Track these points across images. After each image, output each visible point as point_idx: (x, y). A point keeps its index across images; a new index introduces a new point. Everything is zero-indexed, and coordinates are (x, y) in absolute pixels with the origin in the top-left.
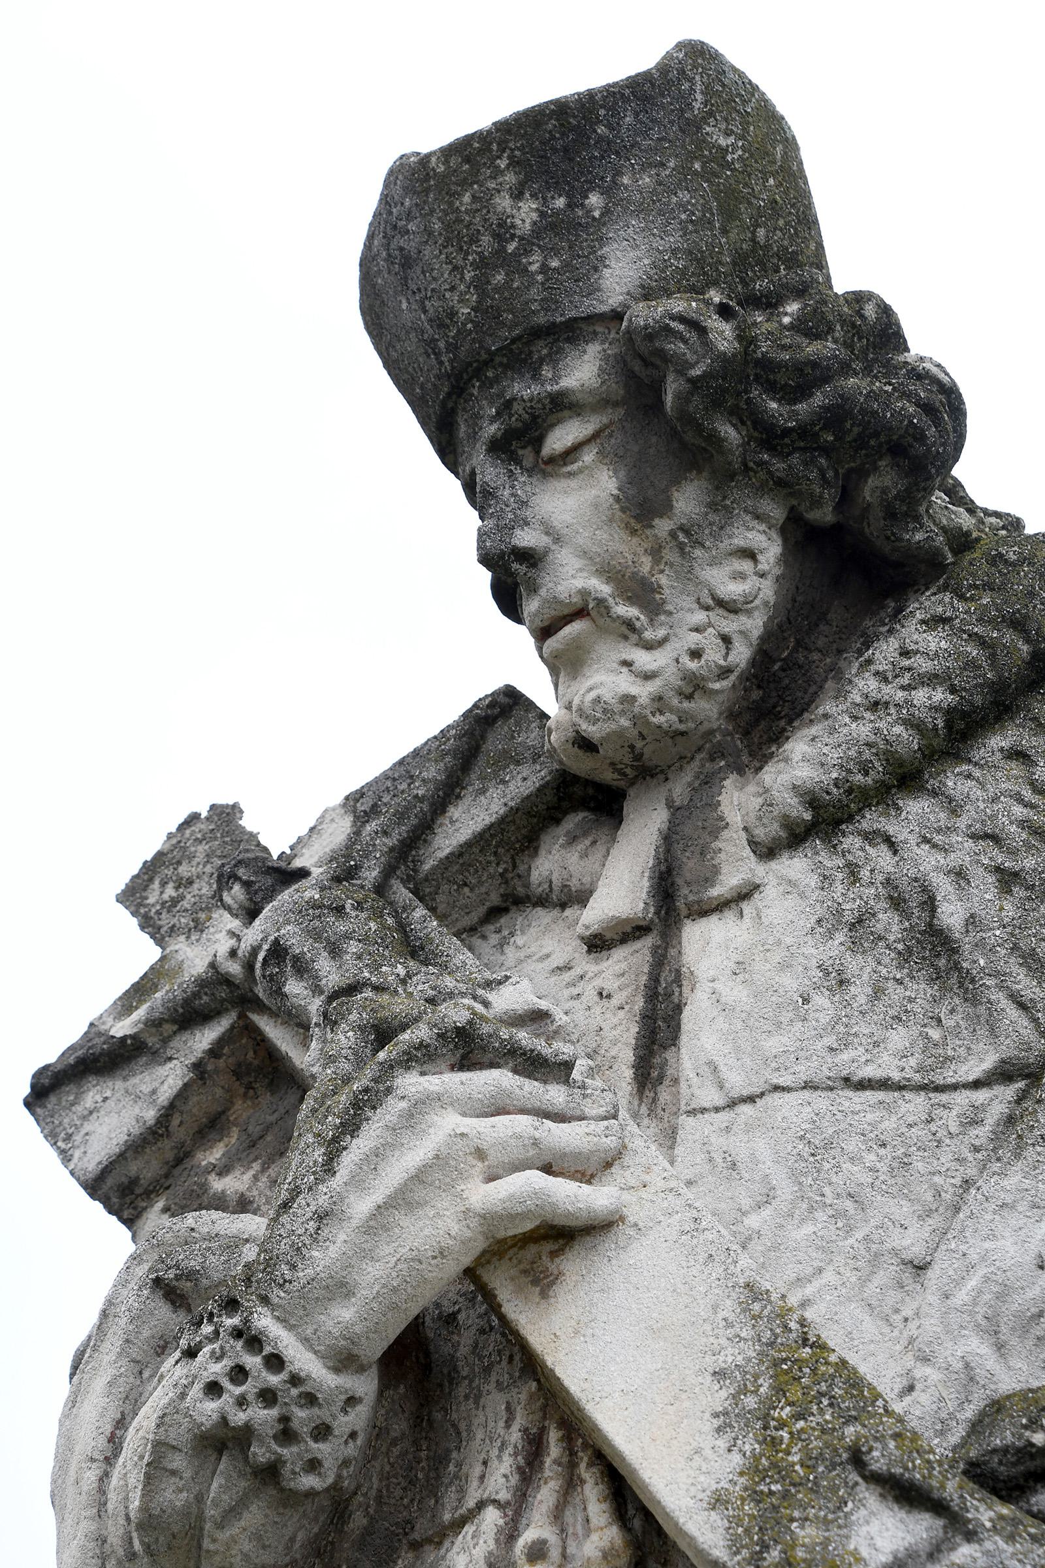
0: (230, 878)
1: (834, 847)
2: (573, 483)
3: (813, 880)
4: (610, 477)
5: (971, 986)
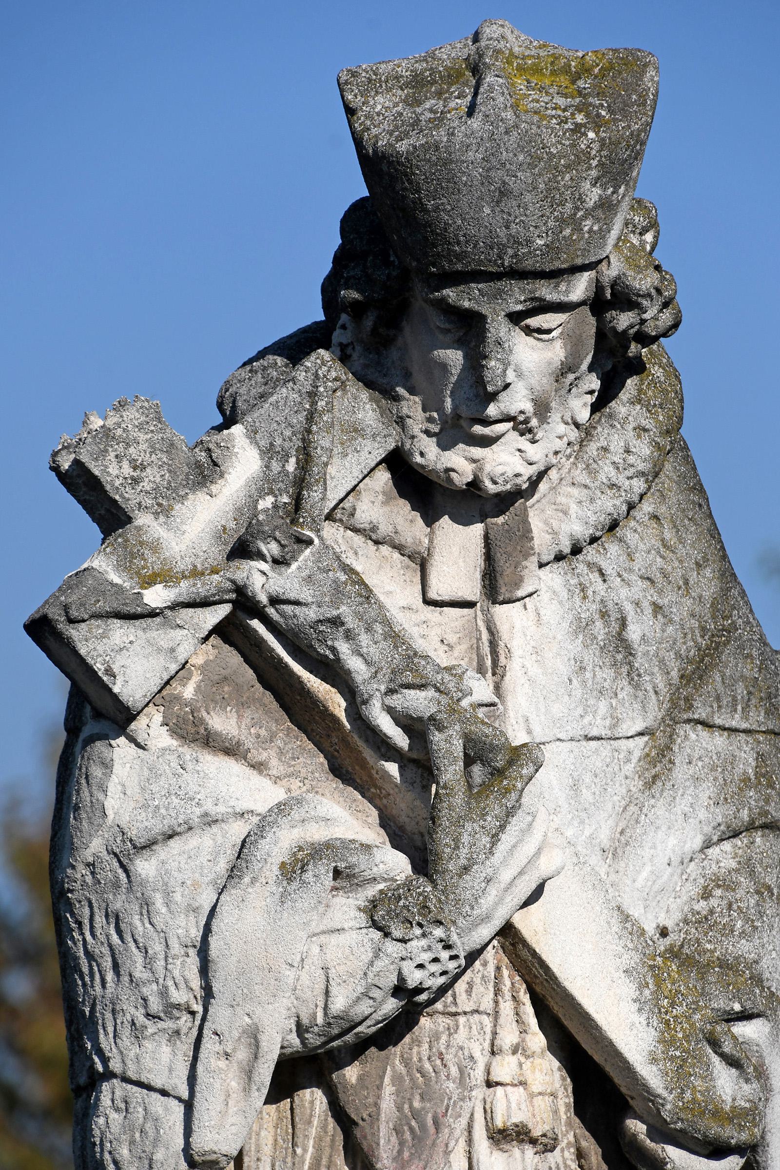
0: (269, 537)
1: (573, 569)
2: (540, 344)
3: (564, 594)
4: (561, 348)
5: (636, 678)
